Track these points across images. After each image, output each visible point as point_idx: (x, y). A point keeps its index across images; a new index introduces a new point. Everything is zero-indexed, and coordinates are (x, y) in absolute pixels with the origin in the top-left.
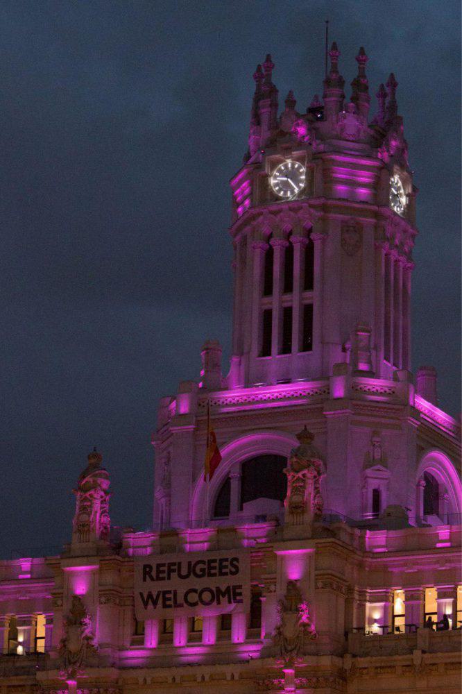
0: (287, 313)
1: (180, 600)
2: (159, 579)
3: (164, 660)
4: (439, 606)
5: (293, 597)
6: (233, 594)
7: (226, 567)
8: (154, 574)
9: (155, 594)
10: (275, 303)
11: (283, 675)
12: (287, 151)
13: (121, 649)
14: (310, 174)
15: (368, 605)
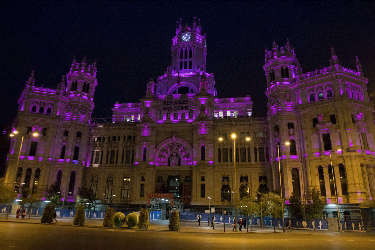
0: (186, 63)
1: (173, 109)
2: (168, 104)
3: (168, 123)
4: (231, 115)
5: (203, 108)
6: (186, 108)
7: (185, 102)
8: (166, 103)
9: (166, 108)
10: (184, 60)
11: (201, 125)
12: (186, 32)
13: (157, 120)
14: (191, 37)
15: (215, 114)
